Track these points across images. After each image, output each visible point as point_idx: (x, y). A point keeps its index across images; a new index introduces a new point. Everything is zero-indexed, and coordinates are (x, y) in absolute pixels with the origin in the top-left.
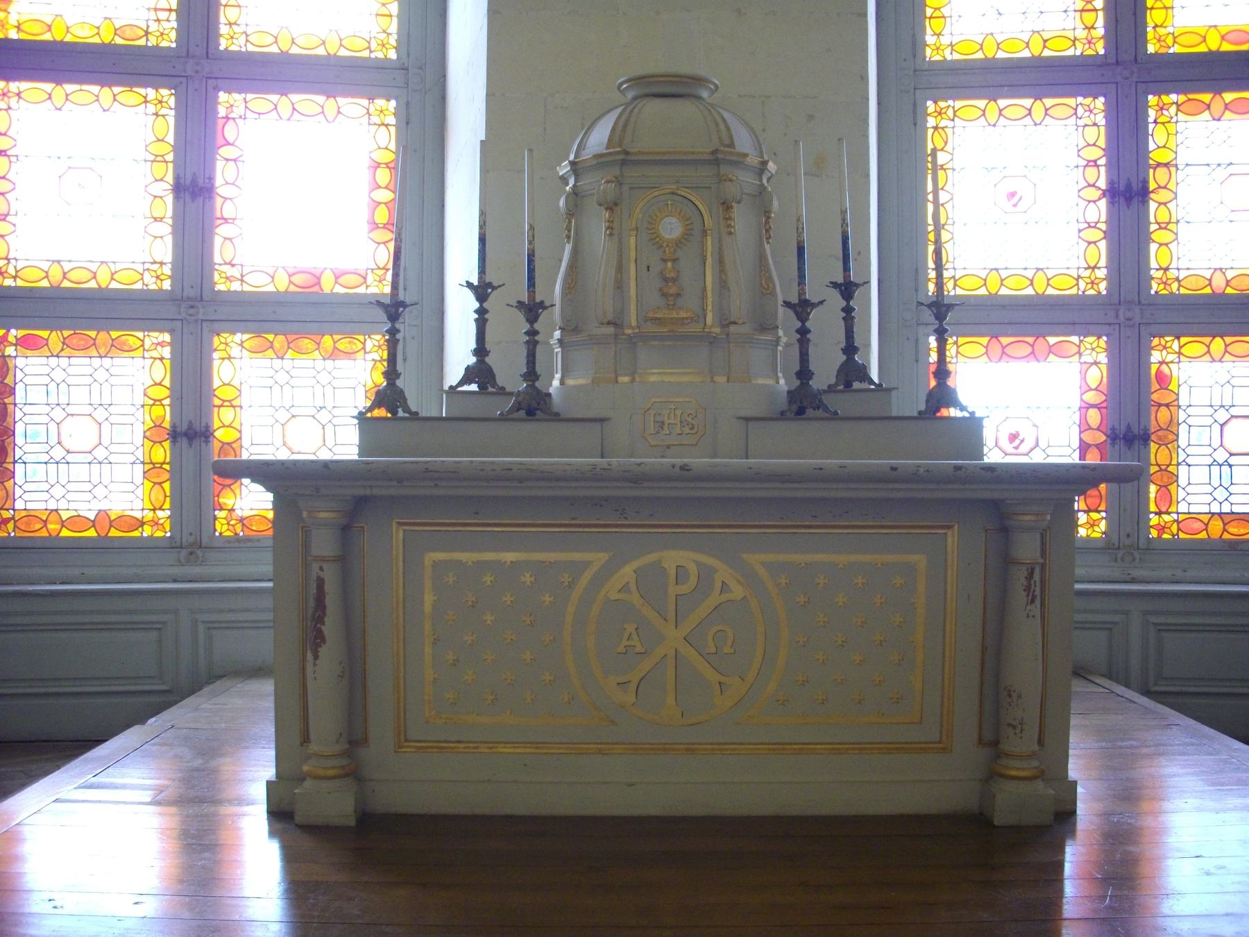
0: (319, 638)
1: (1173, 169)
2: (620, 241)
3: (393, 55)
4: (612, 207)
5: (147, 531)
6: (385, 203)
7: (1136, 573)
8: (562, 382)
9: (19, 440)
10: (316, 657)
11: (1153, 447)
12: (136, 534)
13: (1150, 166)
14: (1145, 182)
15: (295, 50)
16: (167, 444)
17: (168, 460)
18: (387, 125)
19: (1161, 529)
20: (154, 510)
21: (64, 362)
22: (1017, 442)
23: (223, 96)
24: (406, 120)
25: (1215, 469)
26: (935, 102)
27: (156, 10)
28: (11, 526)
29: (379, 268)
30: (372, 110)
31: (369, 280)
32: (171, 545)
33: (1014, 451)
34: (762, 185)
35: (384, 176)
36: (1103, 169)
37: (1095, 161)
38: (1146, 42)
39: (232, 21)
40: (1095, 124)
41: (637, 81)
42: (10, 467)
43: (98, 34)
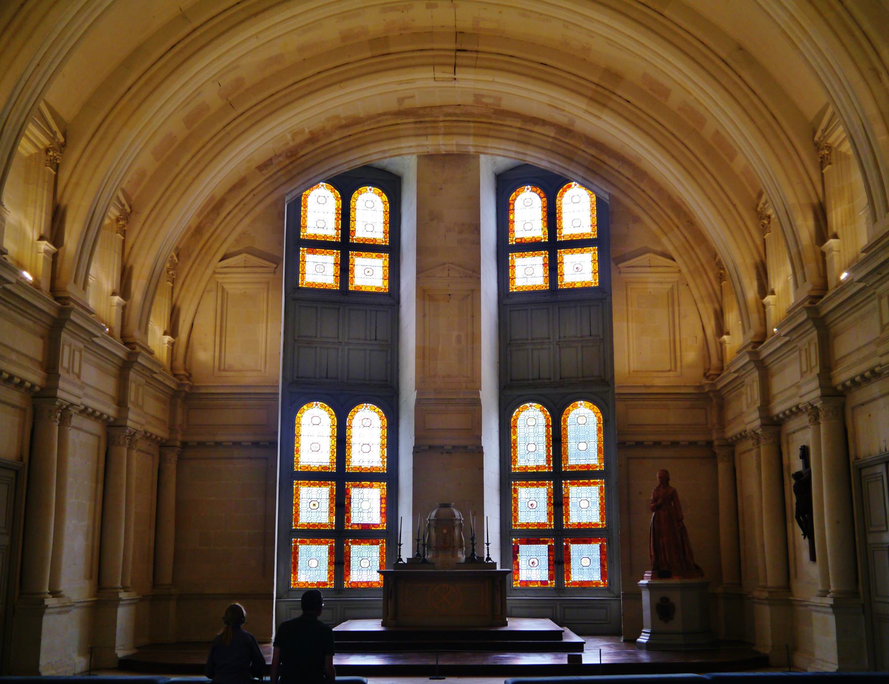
4: (435, 528)
5: (328, 587)
7: (562, 595)
9: (299, 565)
11: (565, 565)
12: (326, 587)
14: (562, 502)
16: (333, 566)
19: (568, 584)
21: (310, 546)
28: (297, 585)
31: (380, 526)
35: (384, 501)
36: (552, 499)
38: (562, 468)
41: (440, 504)
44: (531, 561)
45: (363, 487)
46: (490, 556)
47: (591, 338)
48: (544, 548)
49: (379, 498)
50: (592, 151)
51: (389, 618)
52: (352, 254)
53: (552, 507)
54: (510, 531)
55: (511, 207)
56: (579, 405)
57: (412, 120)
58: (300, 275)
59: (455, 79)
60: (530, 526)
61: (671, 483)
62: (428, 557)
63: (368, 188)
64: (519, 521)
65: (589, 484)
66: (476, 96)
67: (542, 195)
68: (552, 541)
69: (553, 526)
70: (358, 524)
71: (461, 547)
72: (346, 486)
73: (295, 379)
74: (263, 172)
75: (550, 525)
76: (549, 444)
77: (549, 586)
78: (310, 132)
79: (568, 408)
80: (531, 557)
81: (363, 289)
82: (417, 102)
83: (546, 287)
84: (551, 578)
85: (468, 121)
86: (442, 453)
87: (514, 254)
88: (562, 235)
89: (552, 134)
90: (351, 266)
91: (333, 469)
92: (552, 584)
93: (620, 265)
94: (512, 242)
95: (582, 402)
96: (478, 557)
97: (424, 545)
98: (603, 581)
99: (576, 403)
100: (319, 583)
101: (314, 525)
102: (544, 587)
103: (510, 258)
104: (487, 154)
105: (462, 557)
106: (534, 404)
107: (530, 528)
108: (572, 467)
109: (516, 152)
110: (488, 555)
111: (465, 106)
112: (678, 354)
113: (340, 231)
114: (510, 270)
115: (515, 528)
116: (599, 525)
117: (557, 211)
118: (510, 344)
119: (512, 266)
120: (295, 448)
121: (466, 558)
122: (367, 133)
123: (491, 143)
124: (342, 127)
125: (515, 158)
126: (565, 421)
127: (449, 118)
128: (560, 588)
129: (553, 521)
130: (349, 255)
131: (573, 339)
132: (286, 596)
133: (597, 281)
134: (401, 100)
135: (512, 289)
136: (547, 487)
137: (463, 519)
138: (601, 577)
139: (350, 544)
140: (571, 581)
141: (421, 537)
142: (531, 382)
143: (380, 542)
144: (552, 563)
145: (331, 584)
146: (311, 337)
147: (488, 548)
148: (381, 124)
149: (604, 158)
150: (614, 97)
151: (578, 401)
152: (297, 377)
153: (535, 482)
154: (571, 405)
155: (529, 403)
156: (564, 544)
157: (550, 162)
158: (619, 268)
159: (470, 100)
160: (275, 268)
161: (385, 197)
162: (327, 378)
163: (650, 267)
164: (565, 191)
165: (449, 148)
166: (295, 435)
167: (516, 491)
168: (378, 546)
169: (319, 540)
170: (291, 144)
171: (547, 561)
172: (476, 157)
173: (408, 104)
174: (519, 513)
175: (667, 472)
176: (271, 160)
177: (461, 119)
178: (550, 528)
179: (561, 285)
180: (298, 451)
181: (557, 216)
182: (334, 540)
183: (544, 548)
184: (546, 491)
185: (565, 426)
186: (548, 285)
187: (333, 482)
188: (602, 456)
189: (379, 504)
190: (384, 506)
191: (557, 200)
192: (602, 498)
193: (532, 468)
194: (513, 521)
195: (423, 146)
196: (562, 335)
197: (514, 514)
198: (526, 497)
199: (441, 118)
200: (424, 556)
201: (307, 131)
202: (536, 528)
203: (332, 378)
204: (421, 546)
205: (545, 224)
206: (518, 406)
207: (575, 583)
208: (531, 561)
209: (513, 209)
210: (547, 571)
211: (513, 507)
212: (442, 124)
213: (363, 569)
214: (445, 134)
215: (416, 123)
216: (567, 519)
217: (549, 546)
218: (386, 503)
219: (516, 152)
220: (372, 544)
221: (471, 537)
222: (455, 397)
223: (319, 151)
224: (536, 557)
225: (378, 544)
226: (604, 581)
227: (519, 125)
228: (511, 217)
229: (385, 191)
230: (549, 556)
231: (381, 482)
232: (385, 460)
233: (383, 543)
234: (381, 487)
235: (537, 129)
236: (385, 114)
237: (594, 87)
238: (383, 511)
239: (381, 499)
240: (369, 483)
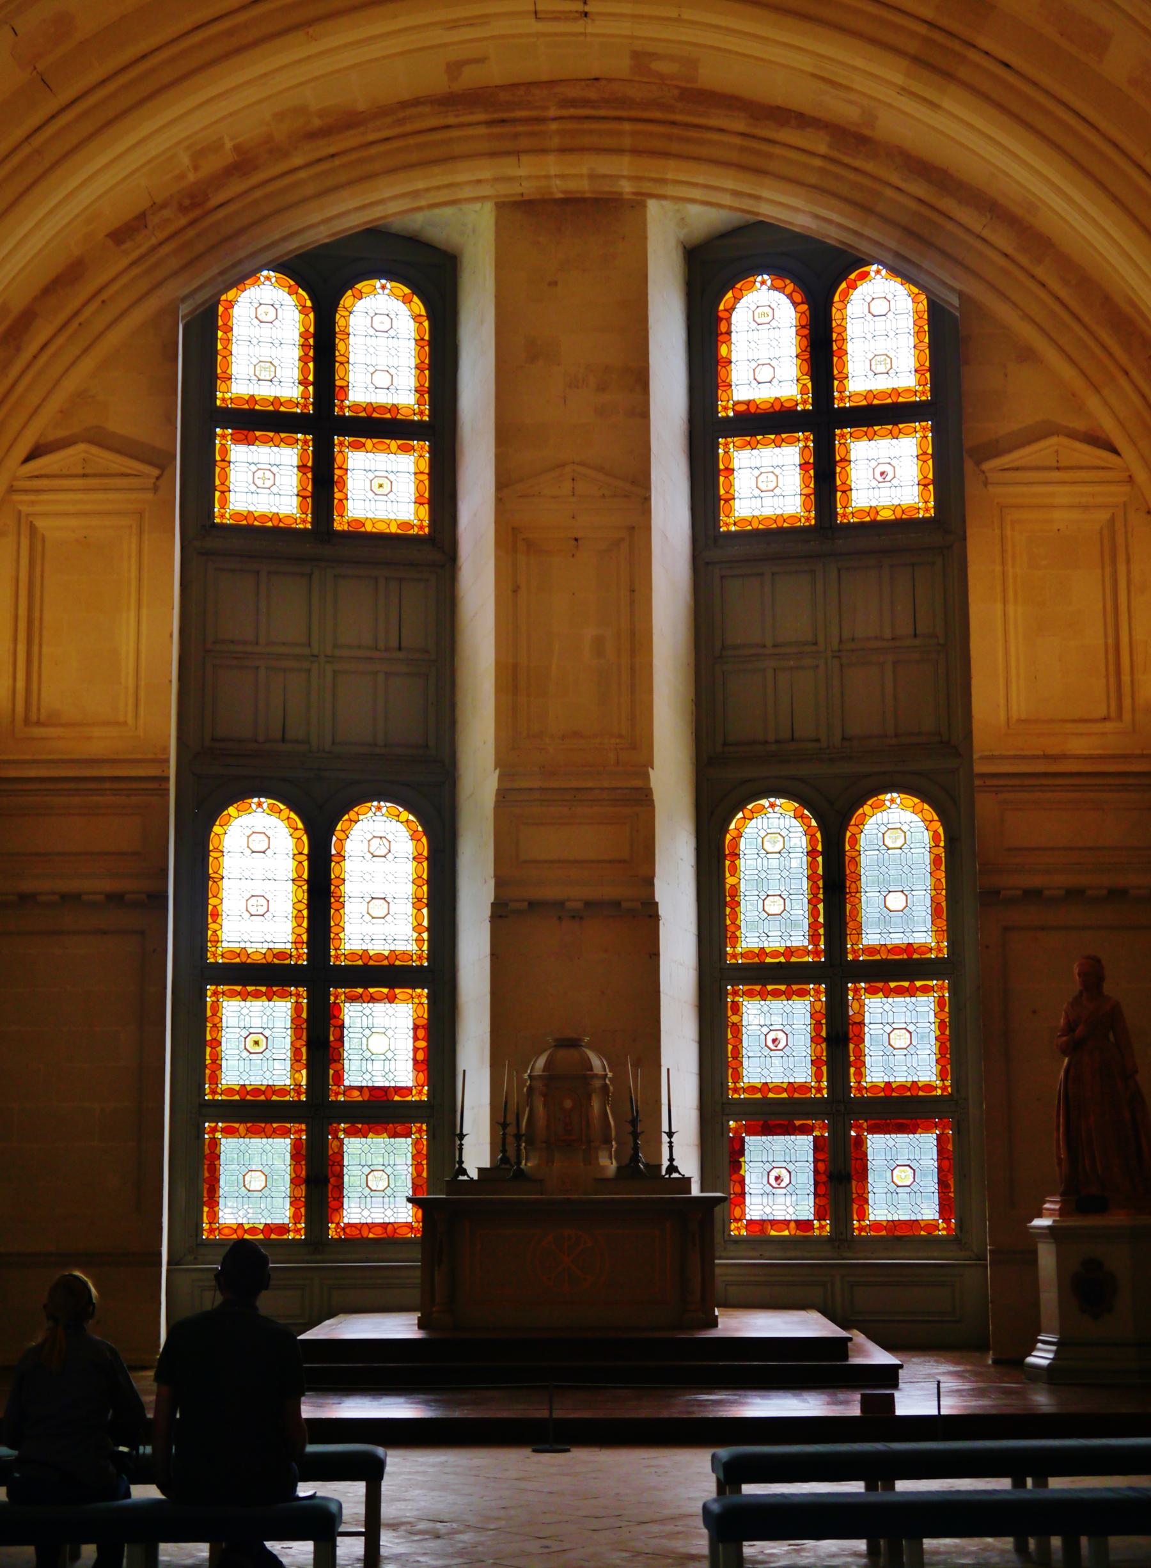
1: (862, 1025)
4: (545, 1095)
5: (291, 1236)
6: (422, 1049)
7: (845, 1254)
8: (526, 1165)
9: (222, 1183)
11: (854, 1183)
12: (285, 1237)
13: (849, 1024)
14: (847, 1033)
16: (303, 1187)
17: (303, 1195)
18: (422, 1004)
19: (861, 1229)
21: (247, 1140)
22: (779, 1181)
25: (889, 1195)
26: (732, 987)
27: (295, 943)
28: (217, 1233)
29: (419, 1086)
30: (414, 995)
31: (414, 1092)
33: (777, 1186)
34: (606, 1085)
35: (421, 1033)
36: (824, 1026)
39: (337, 947)
40: (820, 1000)
41: (556, 1040)
43: (265, 958)
44: (773, 1174)
45: (373, 999)
46: (675, 1163)
47: (917, 642)
48: (803, 1145)
49: (411, 1026)
50: (919, 189)
51: (434, 1309)
52: (341, 444)
53: (824, 1045)
54: (723, 1104)
55: (723, 327)
56: (888, 803)
57: (481, 116)
58: (217, 494)
59: (586, 14)
60: (770, 1090)
61: (1108, 988)
62: (529, 1165)
63: (378, 283)
64: (746, 1080)
65: (911, 992)
66: (636, 55)
67: (798, 297)
68: (822, 1128)
69: (825, 1092)
70: (360, 1089)
71: (607, 1141)
72: (332, 999)
74: (125, 247)
75: (819, 1090)
76: (815, 895)
77: (817, 1232)
78: (237, 148)
79: (861, 811)
80: (774, 1164)
81: (369, 528)
82: (496, 72)
83: (808, 519)
84: (820, 1214)
85: (619, 119)
86: (560, 918)
87: (729, 440)
89: (823, 149)
90: (337, 472)
91: (299, 956)
92: (825, 1228)
93: (986, 466)
94: (725, 412)
95: (895, 795)
96: (646, 1165)
97: (518, 1137)
98: (944, 1221)
99: (881, 797)
101: (257, 1091)
103: (721, 451)
104: (664, 197)
105: (609, 1165)
106: (779, 802)
107: (771, 1095)
108: (871, 950)
109: (736, 193)
110: (671, 1159)
112: (1126, 678)
113: (311, 388)
114: (722, 479)
115: (736, 1096)
116: (935, 1088)
117: (835, 335)
119: (727, 469)
120: (210, 907)
121: (619, 1168)
122: (373, 150)
123: (672, 170)
124: (312, 135)
125: (731, 208)
126: (854, 840)
127: (572, 111)
128: (842, 1238)
129: (825, 1079)
130: (333, 445)
132: (190, 1258)
133: (931, 504)
134: (454, 68)
135: (727, 524)
136: (812, 999)
137: (610, 1075)
138: (942, 1212)
140: (868, 1222)
141: (511, 1119)
142: (774, 747)
143: (414, 1130)
144: (824, 1178)
145: (298, 1231)
147: (670, 1143)
148: (408, 128)
149: (948, 204)
150: (973, 55)
151: (886, 793)
152: (213, 739)
153: (783, 988)
154: (870, 802)
155: (767, 797)
156: (853, 1133)
157: (817, 217)
158: (983, 472)
159: (621, 66)
160: (158, 478)
161: (418, 306)
162: (283, 740)
163: (1058, 468)
165: (572, 185)
166: (208, 877)
167: (736, 1008)
168: (409, 1140)
170: (192, 177)
171: (812, 1174)
172: (637, 204)
173: (471, 78)
175: (1099, 961)
176: (142, 217)
178: (819, 1095)
179: (844, 515)
180: (216, 915)
181: (835, 348)
182: (303, 1127)
183: (803, 1145)
184: (808, 1008)
185: (854, 854)
186: (813, 514)
187: (301, 989)
188: (943, 924)
189: (411, 1041)
190: (422, 1044)
191: (834, 310)
192: (942, 1025)
193: (775, 954)
194: (730, 1080)
195: (510, 179)
196: (846, 634)
197: (734, 1064)
198: (762, 1023)
199: (553, 112)
200: (519, 1163)
201: (229, 145)
202: (785, 1095)
203: (297, 741)
204: (510, 1140)
205: (806, 367)
206: (740, 806)
207: (877, 1225)
208: (773, 1174)
209: (729, 333)
210: (812, 1197)
211: (730, 1047)
212: (554, 126)
213: (372, 1194)
214: (562, 150)
215: (490, 123)
216: (860, 1075)
217: (816, 1139)
218: (428, 1039)
219: (736, 193)
220: (394, 1135)
221: (630, 1117)
222: (590, 784)
223: (258, 194)
224: (784, 1164)
225: (408, 1135)
226: (946, 1220)
227: (741, 125)
228: (723, 350)
229: (418, 289)
230: (816, 1161)
231: (413, 988)
232: (425, 935)
233: (420, 1130)
234: (416, 1001)
235: (786, 135)
236: (416, 102)
237: (922, 29)
238: (421, 1056)
239: (416, 1028)
240: (385, 990)
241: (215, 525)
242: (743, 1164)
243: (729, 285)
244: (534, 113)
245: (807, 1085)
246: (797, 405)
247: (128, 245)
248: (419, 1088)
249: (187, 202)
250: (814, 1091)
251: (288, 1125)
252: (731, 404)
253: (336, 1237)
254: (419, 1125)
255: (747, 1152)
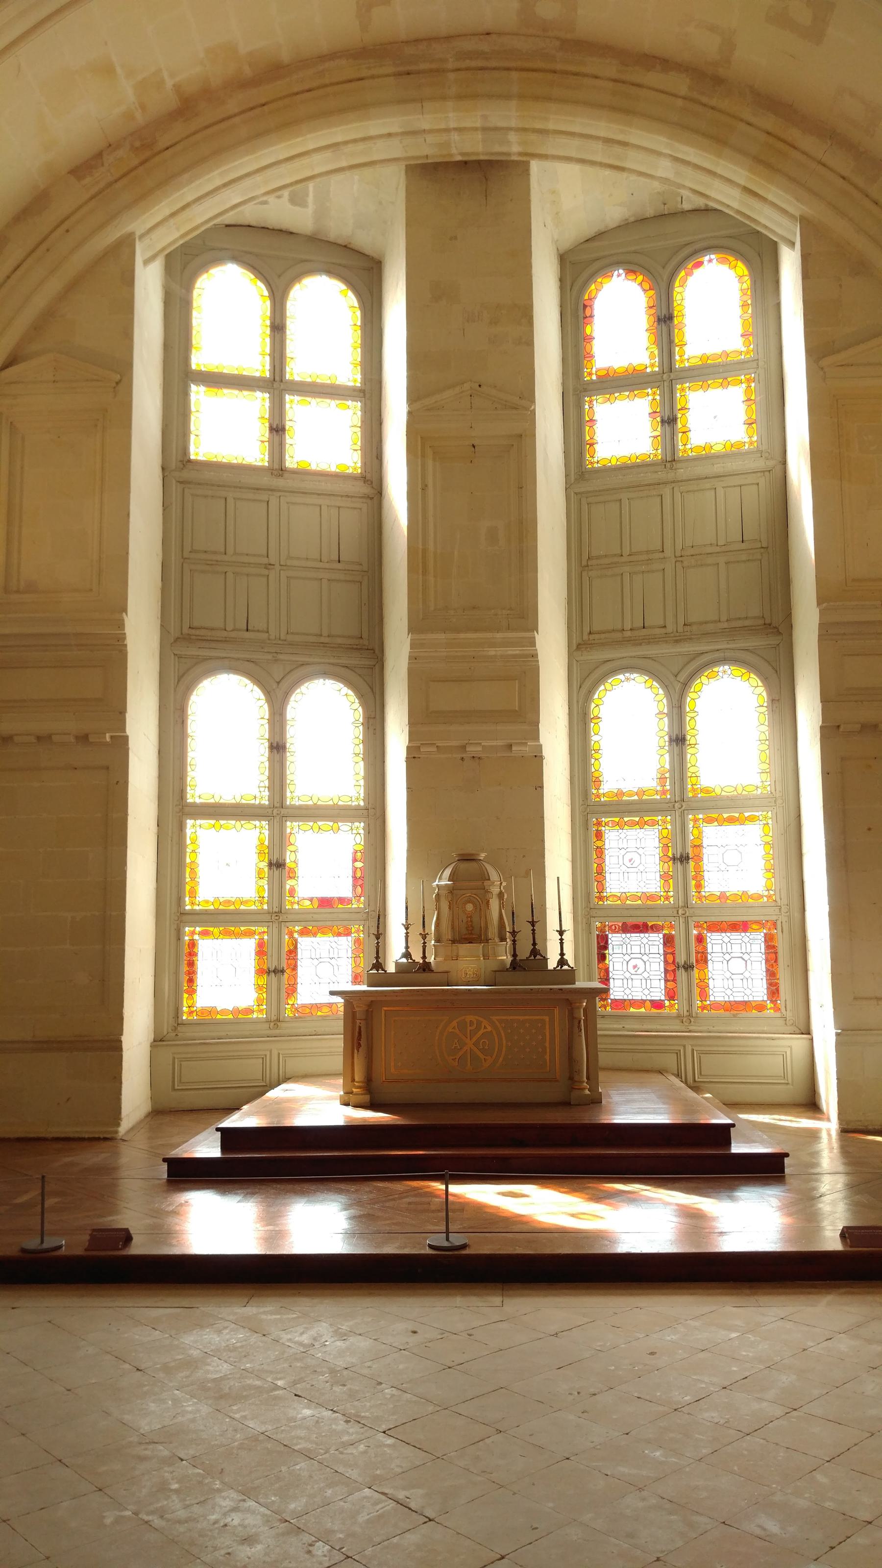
0: (359, 1045)
2: (453, 912)
3: (362, 803)
5: (255, 1015)
7: (691, 1028)
10: (358, 1052)
12: (250, 1016)
15: (319, 803)
17: (265, 983)
20: (259, 1006)
22: (636, 969)
23: (288, 824)
24: (368, 831)
26: (597, 819)
28: (195, 1014)
32: (268, 1021)
33: (635, 973)
37: (667, 845)
40: (667, 828)
41: (460, 855)
42: (195, 988)
47: (743, 546)
55: (588, 313)
70: (311, 900)
73: (186, 630)
77: (667, 1010)
80: (632, 956)
84: (671, 995)
85: (508, 69)
88: (686, 357)
89: (683, 90)
95: (726, 667)
98: (772, 1002)
99: (716, 669)
100: (236, 1011)
101: (228, 902)
102: (657, 1013)
103: (587, 407)
111: (499, 34)
113: (268, 359)
116: (762, 897)
118: (588, 566)
127: (468, 63)
131: (709, 550)
136: (660, 828)
139: (296, 935)
140: (708, 1002)
143: (353, 930)
146: (215, 553)
149: (794, 134)
151: (719, 665)
154: (706, 674)
160: (117, 383)
164: (689, 274)
169: (237, 929)
174: (607, 875)
176: (99, 155)
177: (494, 64)
178: (667, 902)
181: (676, 322)
182: (266, 930)
186: (659, 451)
190: (359, 865)
199: (450, 65)
201: (169, 83)
212: (452, 76)
217: (664, 935)
225: (348, 934)
228: (588, 330)
230: (665, 954)
234: (355, 831)
235: (654, 78)
236: (333, 56)
241: (189, 461)
242: (607, 955)
243: (591, 278)
244: (434, 66)
245: (656, 894)
246: (646, 368)
247: (88, 180)
248: (358, 898)
249: (137, 144)
250: (662, 899)
251: (253, 928)
252: (594, 371)
253: (291, 1015)
254: (357, 926)
255: (610, 947)
